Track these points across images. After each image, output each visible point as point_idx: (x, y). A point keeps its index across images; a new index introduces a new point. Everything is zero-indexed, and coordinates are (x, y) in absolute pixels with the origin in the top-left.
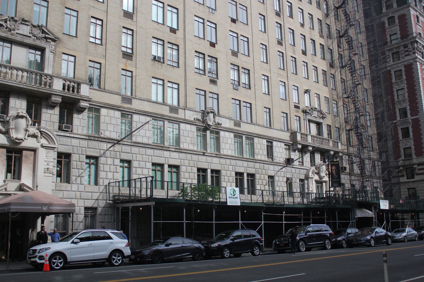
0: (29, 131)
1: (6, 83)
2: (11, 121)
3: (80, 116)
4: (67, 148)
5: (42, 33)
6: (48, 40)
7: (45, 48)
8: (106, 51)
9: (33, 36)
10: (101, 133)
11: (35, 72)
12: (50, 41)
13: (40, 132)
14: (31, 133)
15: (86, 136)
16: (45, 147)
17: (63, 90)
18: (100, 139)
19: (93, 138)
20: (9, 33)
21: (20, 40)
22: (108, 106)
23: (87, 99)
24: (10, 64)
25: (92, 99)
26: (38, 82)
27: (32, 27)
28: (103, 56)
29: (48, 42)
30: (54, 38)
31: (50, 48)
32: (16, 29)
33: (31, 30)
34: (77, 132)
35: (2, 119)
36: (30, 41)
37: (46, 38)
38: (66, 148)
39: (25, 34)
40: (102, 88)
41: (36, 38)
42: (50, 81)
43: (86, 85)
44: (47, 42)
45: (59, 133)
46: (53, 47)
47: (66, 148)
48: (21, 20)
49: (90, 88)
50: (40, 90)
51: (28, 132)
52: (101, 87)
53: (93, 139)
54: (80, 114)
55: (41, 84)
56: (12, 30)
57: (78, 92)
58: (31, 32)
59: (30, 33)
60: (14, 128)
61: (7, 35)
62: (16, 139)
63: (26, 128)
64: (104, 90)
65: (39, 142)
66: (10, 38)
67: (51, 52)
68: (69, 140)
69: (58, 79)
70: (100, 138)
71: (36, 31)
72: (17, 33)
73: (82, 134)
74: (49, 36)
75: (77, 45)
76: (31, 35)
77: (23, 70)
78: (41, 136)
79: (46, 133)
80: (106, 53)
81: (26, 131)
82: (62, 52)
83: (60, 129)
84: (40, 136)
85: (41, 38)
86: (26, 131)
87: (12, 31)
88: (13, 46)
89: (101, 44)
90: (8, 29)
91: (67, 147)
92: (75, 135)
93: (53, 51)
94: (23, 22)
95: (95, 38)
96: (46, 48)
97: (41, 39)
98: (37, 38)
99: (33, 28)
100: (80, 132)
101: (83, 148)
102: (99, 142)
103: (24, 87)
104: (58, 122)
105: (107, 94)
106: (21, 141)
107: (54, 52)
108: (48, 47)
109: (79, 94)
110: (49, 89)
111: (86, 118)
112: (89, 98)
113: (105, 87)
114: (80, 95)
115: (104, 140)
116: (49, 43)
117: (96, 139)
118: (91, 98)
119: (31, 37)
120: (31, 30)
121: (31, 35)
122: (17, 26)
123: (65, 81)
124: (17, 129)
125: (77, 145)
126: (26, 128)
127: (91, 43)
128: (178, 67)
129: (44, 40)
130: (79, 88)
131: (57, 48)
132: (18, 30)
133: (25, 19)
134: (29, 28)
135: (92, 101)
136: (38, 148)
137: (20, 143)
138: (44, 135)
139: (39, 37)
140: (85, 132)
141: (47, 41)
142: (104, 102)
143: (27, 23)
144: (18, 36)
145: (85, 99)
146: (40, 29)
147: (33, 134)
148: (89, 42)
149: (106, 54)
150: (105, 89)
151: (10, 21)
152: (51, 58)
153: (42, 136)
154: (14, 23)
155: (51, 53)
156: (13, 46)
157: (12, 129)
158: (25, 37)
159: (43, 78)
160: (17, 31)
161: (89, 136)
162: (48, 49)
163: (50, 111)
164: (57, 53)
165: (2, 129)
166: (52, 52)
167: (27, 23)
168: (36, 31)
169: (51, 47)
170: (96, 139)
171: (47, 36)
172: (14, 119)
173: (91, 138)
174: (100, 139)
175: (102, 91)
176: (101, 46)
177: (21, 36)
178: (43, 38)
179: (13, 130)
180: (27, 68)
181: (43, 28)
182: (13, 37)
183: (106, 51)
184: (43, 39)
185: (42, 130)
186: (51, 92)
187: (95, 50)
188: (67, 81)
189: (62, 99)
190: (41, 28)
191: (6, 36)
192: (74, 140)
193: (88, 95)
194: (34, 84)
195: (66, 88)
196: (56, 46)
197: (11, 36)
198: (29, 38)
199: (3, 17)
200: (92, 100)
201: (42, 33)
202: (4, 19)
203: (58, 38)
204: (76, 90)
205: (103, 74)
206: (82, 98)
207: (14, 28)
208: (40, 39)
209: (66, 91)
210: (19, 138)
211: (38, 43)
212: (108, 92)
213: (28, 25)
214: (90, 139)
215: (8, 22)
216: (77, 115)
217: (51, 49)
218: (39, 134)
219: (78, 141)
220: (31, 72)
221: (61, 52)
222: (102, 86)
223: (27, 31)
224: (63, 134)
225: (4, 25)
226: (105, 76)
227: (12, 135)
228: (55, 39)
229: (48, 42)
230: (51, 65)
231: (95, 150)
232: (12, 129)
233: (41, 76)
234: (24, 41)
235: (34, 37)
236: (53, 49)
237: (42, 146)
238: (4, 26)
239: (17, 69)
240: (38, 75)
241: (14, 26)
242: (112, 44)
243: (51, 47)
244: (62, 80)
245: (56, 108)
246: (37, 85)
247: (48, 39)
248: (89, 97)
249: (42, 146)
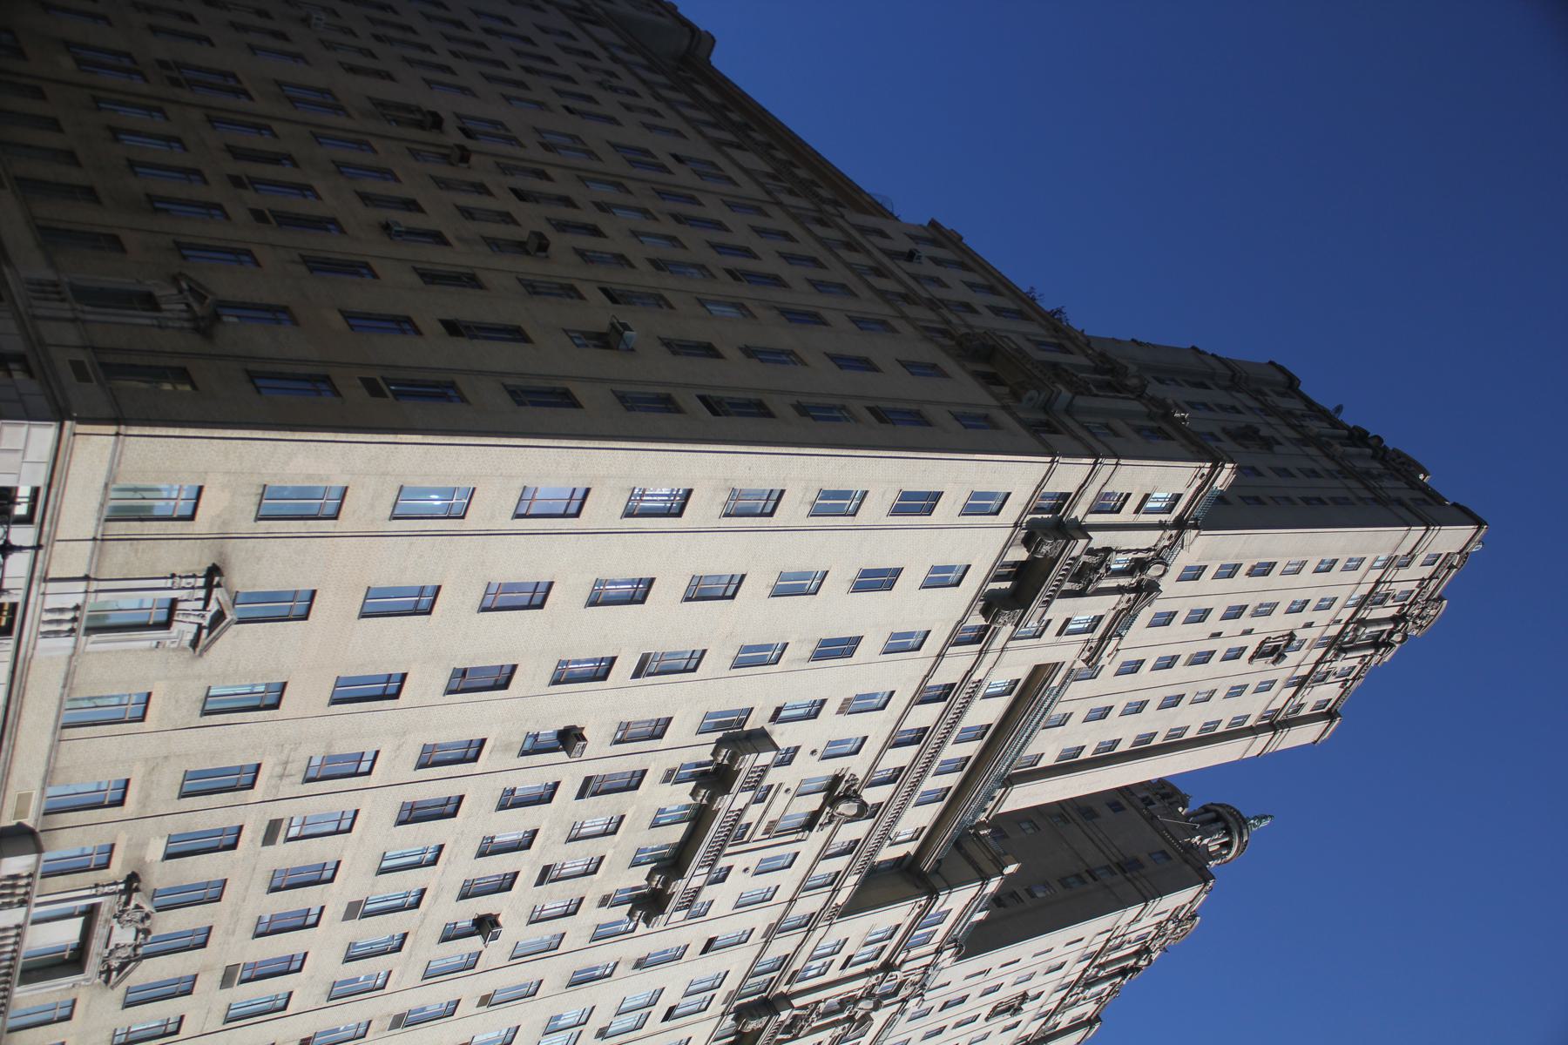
9: (111, 951)
20: (109, 916)
76: (112, 946)
88: (81, 919)
119: (107, 947)
121: (112, 946)
141: (101, 973)
146: (128, 957)
150: (60, 741)
160: (117, 927)
171: (114, 973)
175: (54, 733)
213: (136, 939)
221: (116, 839)
222: (68, 733)
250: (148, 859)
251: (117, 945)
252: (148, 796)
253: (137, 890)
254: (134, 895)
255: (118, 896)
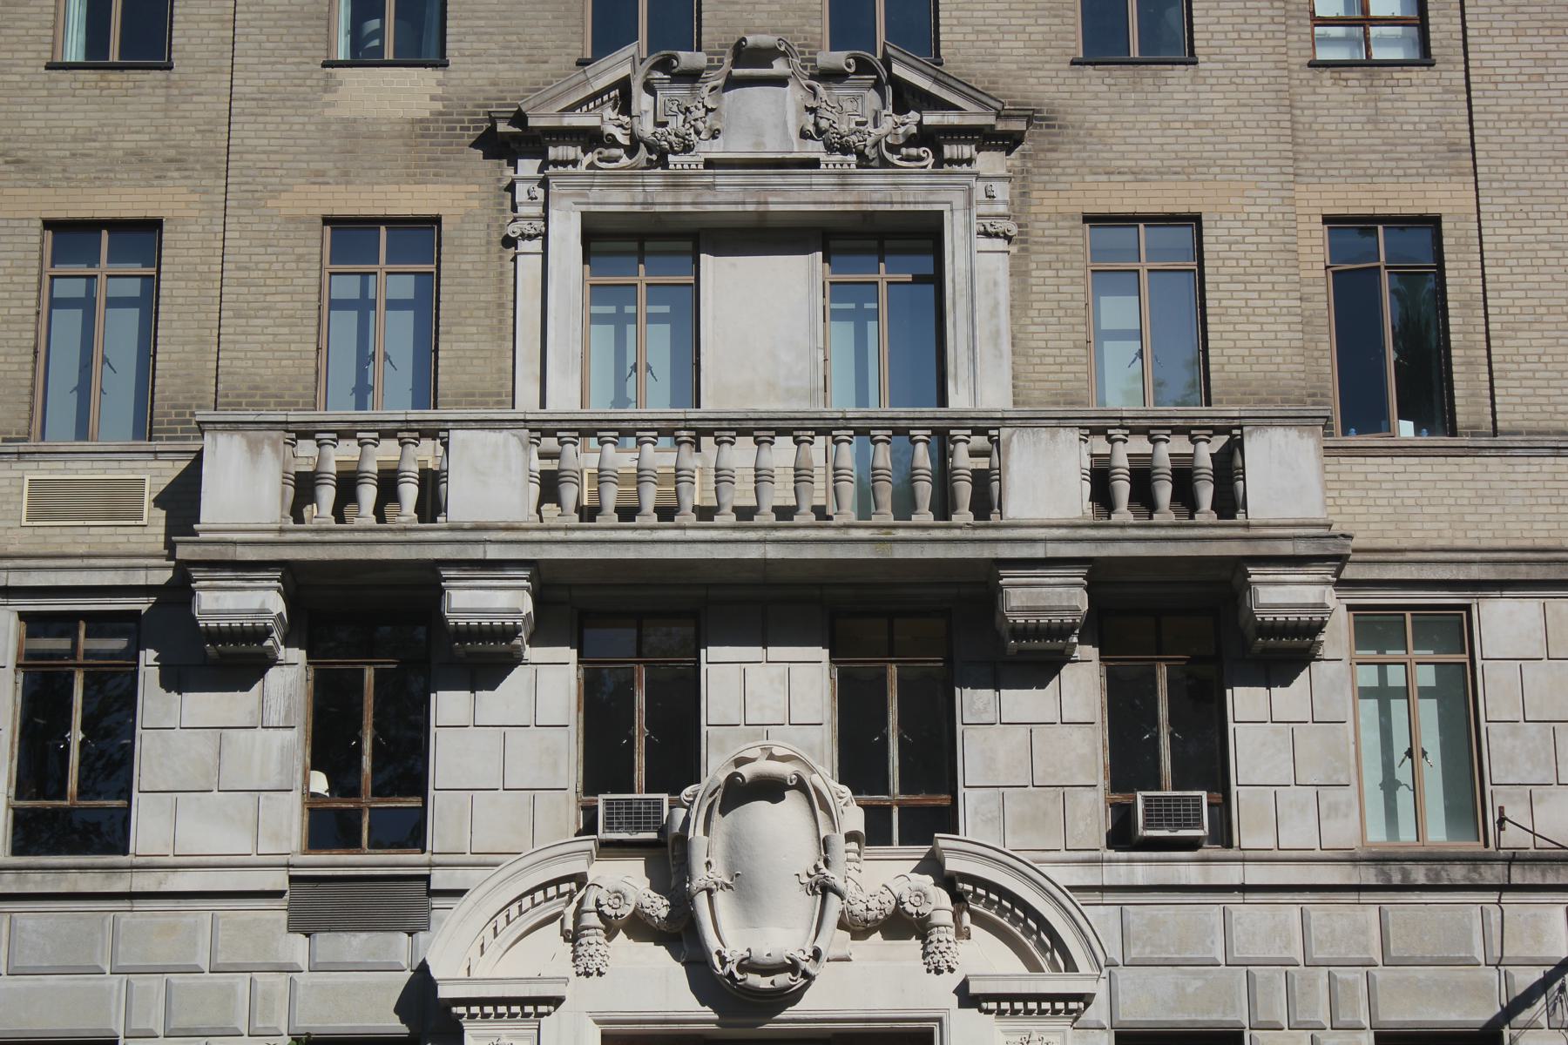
0: (841, 895)
1: (631, 553)
2: (696, 833)
3: (1290, 698)
4: (1199, 983)
5: (901, 108)
6: (949, 151)
7: (939, 215)
8: (1470, 107)
9: (830, 148)
10: (1502, 821)
11: (854, 424)
12: (967, 151)
13: (948, 882)
14: (873, 904)
15: (1354, 860)
16: (993, 1006)
17: (291, 524)
18: (1492, 874)
19: (1419, 875)
20: (655, 177)
21: (740, 208)
22: (1538, 573)
23: (1303, 549)
24: (698, 406)
25: (1350, 537)
26: (925, 490)
27: (814, 83)
28: (1453, 148)
29: (951, 162)
30: (991, 120)
31: (969, 203)
32: (698, 133)
33: (812, 110)
34: (1271, 844)
35: (647, 829)
36: (808, 196)
37: (929, 138)
38: (1190, 990)
39: (773, 148)
40: (1473, 420)
41: (853, 158)
42: (983, 463)
43: (1293, 433)
44: (946, 168)
45: (1106, 868)
46: (1002, 191)
47: (1190, 990)
48: (728, 60)
49: (1329, 451)
50: (900, 553)
51: (833, 899)
52: (1461, 419)
53: (1422, 880)
54: (1286, 683)
55: (944, 506)
56: (675, 153)
57: (1229, 503)
58: (811, 128)
59: (804, 135)
60: (728, 886)
61: (640, 199)
62: (742, 968)
63: (816, 868)
64: (1484, 442)
65: (938, 972)
66: (669, 209)
67: (987, 234)
68: (1210, 912)
69: (1044, 434)
70: (1488, 860)
71: (848, 106)
72: (709, 164)
73: (1318, 853)
74: (952, 119)
75: (1197, 125)
76: (814, 149)
77: (825, 428)
78: (957, 917)
79: (990, 886)
80: (1471, 121)
81: (824, 889)
82: (1080, 210)
83: (1122, 836)
84: (946, 917)
85: (893, 149)
86: (824, 889)
87: (671, 158)
88: (705, 259)
89: (1425, 59)
90: (643, 153)
91: (1193, 981)
92: (1250, 867)
93: (1002, 226)
94: (737, 72)
95: (1366, 21)
96: (947, 215)
97: (894, 159)
98: (861, 155)
99: (820, 88)
100: (1299, 834)
101: (1341, 973)
102: (1493, 897)
103: (773, 552)
104: (1102, 781)
105: (1523, 467)
106: (782, 979)
107: (1014, 231)
108: (959, 199)
109: (1240, 517)
110: (975, 527)
111: (1342, 704)
112: (1335, 529)
113: (1494, 413)
114: (1247, 526)
115: (1534, 877)
116: (965, 168)
117: (1458, 874)
118: (1347, 530)
119: (814, 163)
120: (812, 110)
121: (814, 149)
122: (702, 112)
123: (1154, 441)
124: (741, 883)
125: (1286, 954)
126: (816, 868)
127: (1327, 74)
128: (1425, 59)
129: (920, 159)
130: (1228, 468)
131: (1035, 194)
132: (714, 134)
133: (751, 40)
134: (793, 95)
135: (1355, 551)
136: (939, 1020)
137: (794, 996)
138: (979, 908)
139: (876, 144)
140: (1342, 833)
141: (940, 162)
142: (1501, 543)
143: (779, 67)
144: (719, 180)
145: (1286, 549)
146: (878, 86)
147: (889, 908)
148: (1308, 74)
149: (1472, 130)
151: (649, 88)
152: (996, 284)
153: (966, 917)
154: (681, 92)
155: (985, 243)
156: (705, 259)
157: (710, 892)
158: (773, 178)
159: (962, 451)
161: (1379, 860)
162: (959, 217)
163: (1020, 702)
164: (1037, 230)
165: (647, 902)
166: (997, 235)
167: (779, 67)
168: (848, 106)
169: (979, 194)
170: (1458, 874)
171: (931, 119)
172: (716, 814)
173: (1405, 874)
174: (1492, 874)
176: (1417, 74)
177: (738, 177)
178: (911, 141)
179: (720, 898)
180: (841, 403)
181: (897, 70)
182: (685, 202)
183: (1469, 100)
184: (913, 151)
185: (952, 864)
186: (987, 552)
187: (1373, 121)
188: (1118, 434)
189: (1088, 589)
190: (884, 75)
191: (637, 208)
192: (1251, 916)
193: (1316, 512)
194: (891, 520)
195: (1123, 489)
196: (1021, 182)
197: (669, 197)
198: (799, 177)
199: (597, 76)
200: (1354, 543)
201: (901, 108)
202: (607, 90)
203: (1031, 117)
204: (1206, 494)
205: (1465, 305)
206: (1263, 549)
207: (682, 131)
208: (885, 163)
209: (1123, 512)
210: (769, 960)
211: (877, 197)
212: (1532, 451)
213: (781, 81)
214: (1397, 879)
215: (642, 101)
216: (1264, 689)
217: (983, 209)
218: (942, 898)
219: (1289, 912)
220: (859, 432)
223: (785, 123)
224: (1140, 869)
225: (610, 129)
226: (1486, 316)
227: (713, 943)
228: (1001, 126)
229: (951, 162)
230: (995, 336)
231: (1461, 973)
232: (710, 892)
233: (942, 440)
234: (772, 208)
235: (838, 157)
236: (1002, 209)
237: (967, 998)
238: (614, 143)
239: (762, 429)
240: (920, 434)
241: (681, 117)
242: (1518, 32)
243: (979, 194)
244: (1075, 435)
245: (1066, 671)
246: (875, 520)
247: (951, 142)
248: (1329, 526)
249: (967, 998)
250: (423, 108)
251: (804, 135)
252: (139, 157)
253: (519, 118)
254: (532, 122)
255: (551, 169)
